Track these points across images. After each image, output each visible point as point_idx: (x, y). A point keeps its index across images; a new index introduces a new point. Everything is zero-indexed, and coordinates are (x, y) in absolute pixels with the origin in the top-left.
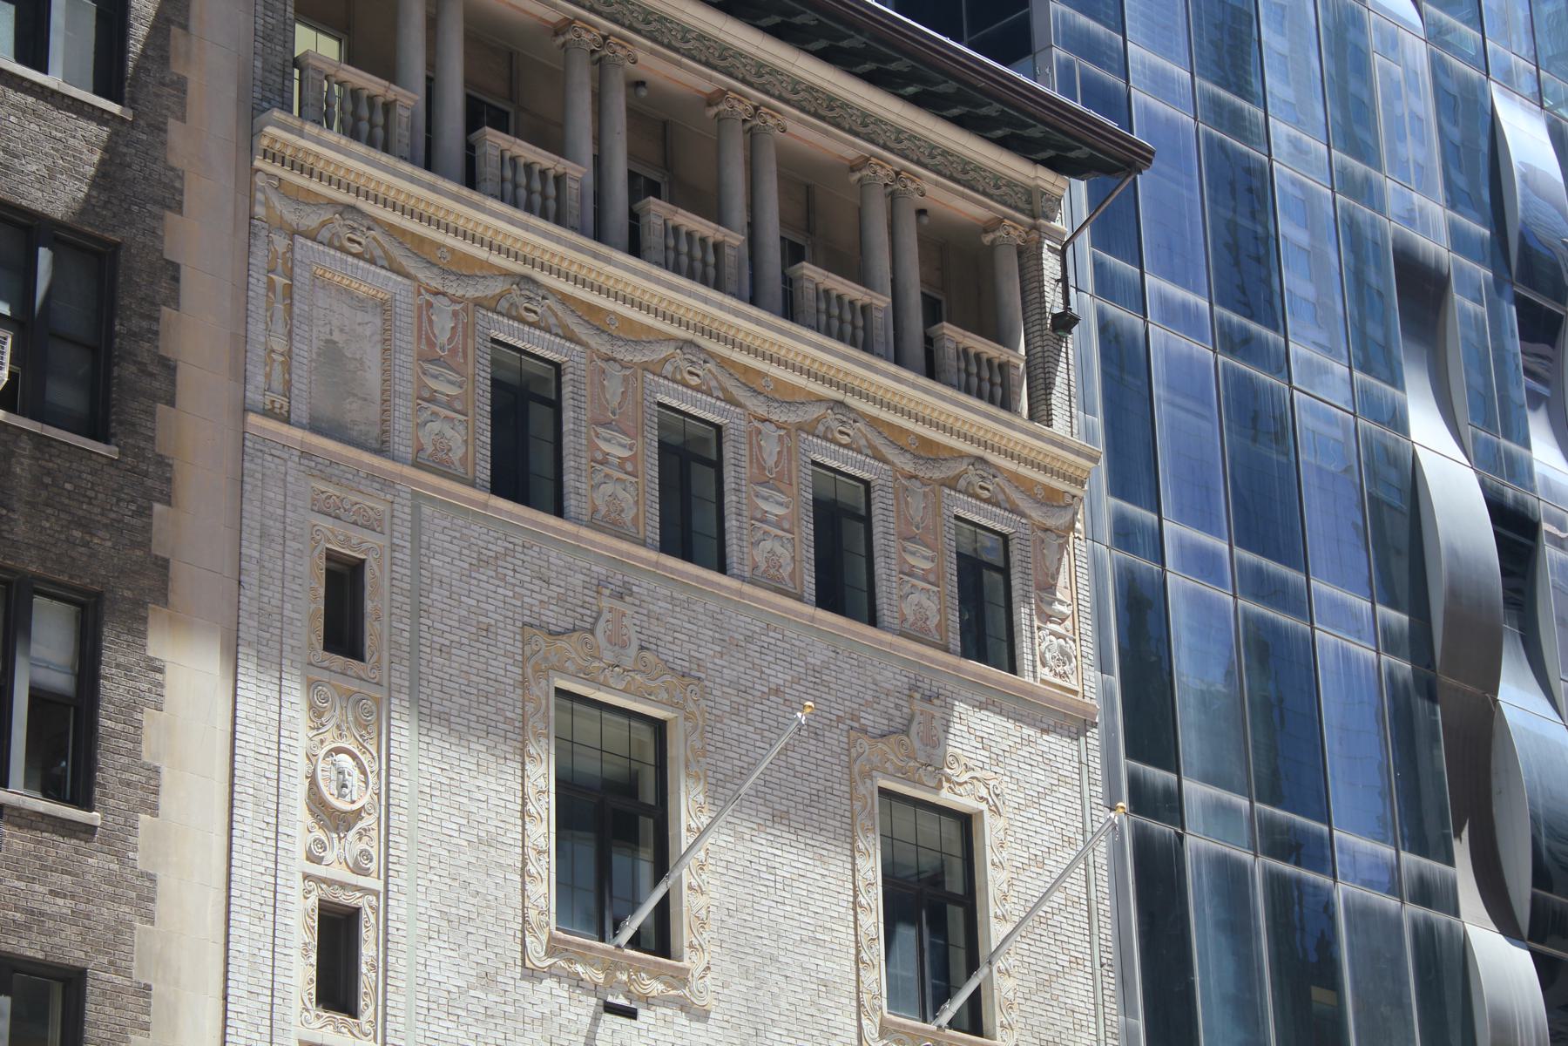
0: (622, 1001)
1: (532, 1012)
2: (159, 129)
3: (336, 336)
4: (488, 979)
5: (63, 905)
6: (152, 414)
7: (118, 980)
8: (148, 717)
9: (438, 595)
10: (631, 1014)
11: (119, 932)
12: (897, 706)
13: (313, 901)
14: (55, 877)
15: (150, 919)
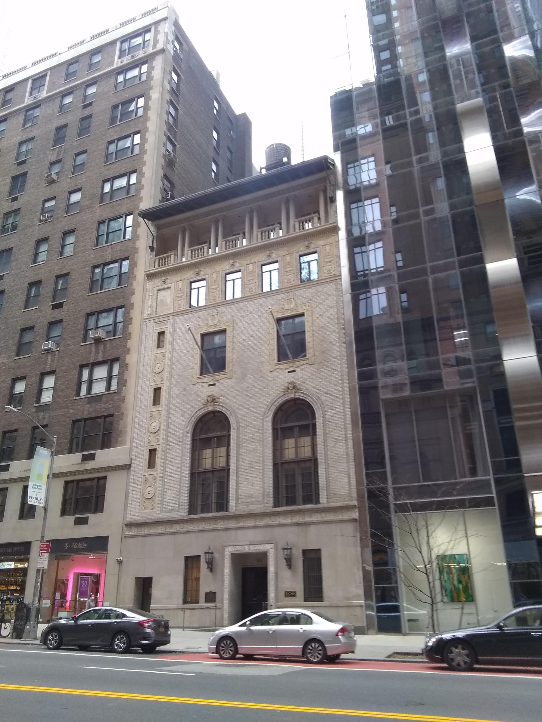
0: (212, 383)
1: (193, 392)
2: (132, 284)
3: (162, 298)
4: (185, 390)
5: (111, 406)
6: (128, 328)
7: (118, 413)
8: (126, 373)
9: (178, 330)
10: (214, 385)
11: (119, 406)
12: (282, 302)
13: (153, 389)
14: (110, 402)
15: (124, 402)
